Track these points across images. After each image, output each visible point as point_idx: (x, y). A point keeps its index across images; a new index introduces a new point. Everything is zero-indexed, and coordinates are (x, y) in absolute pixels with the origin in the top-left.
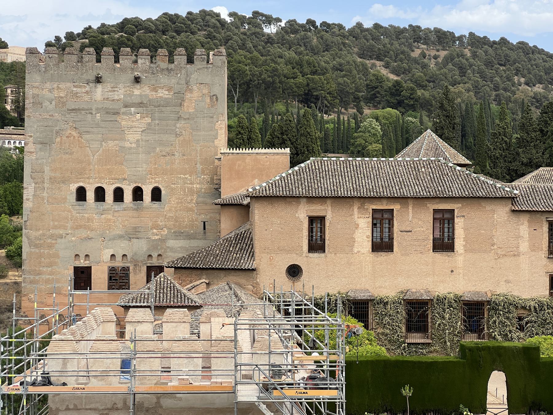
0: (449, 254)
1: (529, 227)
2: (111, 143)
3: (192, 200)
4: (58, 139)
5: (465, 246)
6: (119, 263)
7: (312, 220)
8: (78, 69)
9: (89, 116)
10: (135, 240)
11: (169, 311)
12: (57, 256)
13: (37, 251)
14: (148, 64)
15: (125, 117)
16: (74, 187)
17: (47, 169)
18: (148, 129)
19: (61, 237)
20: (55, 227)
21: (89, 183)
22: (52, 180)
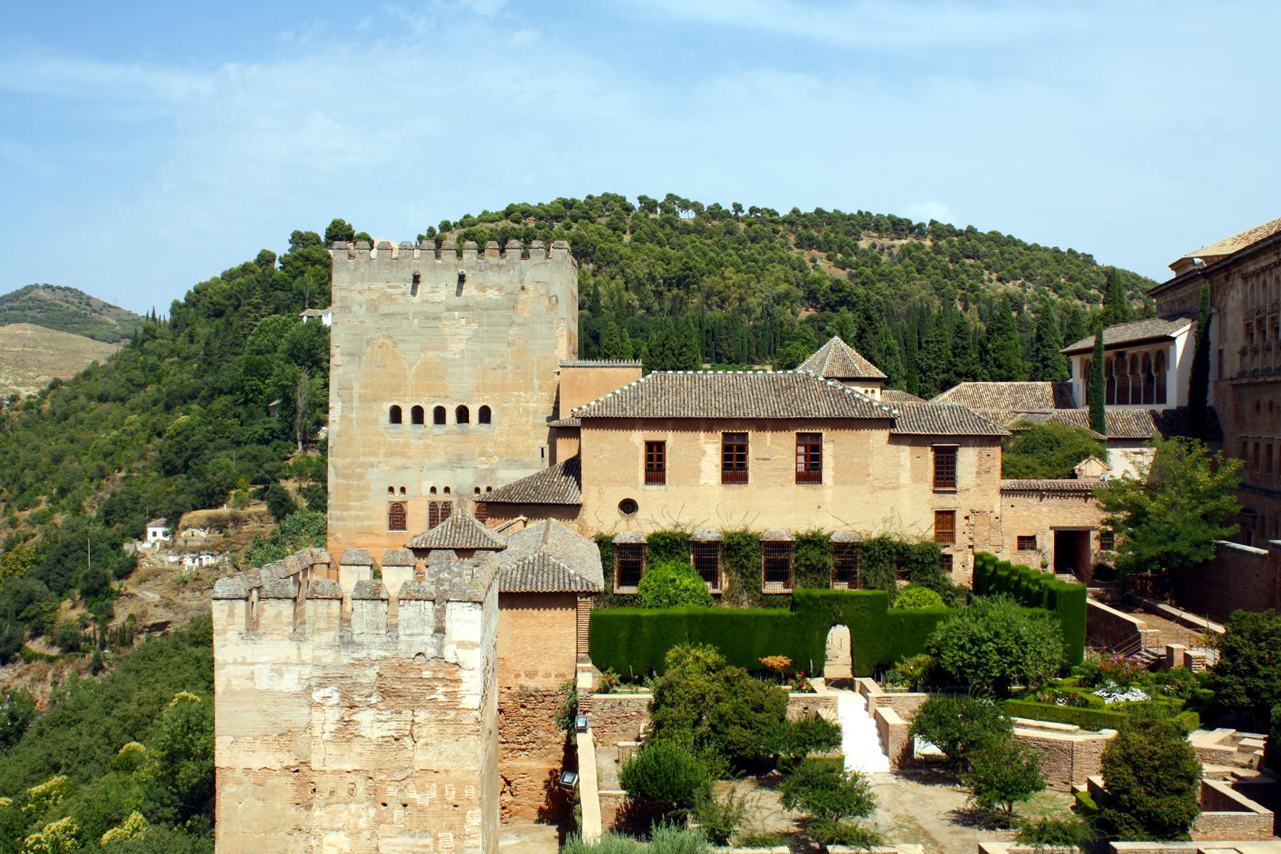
0: (815, 486)
1: (911, 454)
2: (430, 354)
3: (527, 422)
4: (369, 349)
5: (834, 477)
6: (441, 497)
7: (650, 445)
8: (393, 266)
9: (405, 321)
10: (459, 471)
11: (477, 552)
12: (368, 488)
13: (345, 482)
14: (475, 259)
15: (446, 323)
16: (387, 407)
17: (356, 385)
18: (475, 337)
19: (372, 466)
20: (365, 454)
21: (404, 402)
22: (363, 398)
